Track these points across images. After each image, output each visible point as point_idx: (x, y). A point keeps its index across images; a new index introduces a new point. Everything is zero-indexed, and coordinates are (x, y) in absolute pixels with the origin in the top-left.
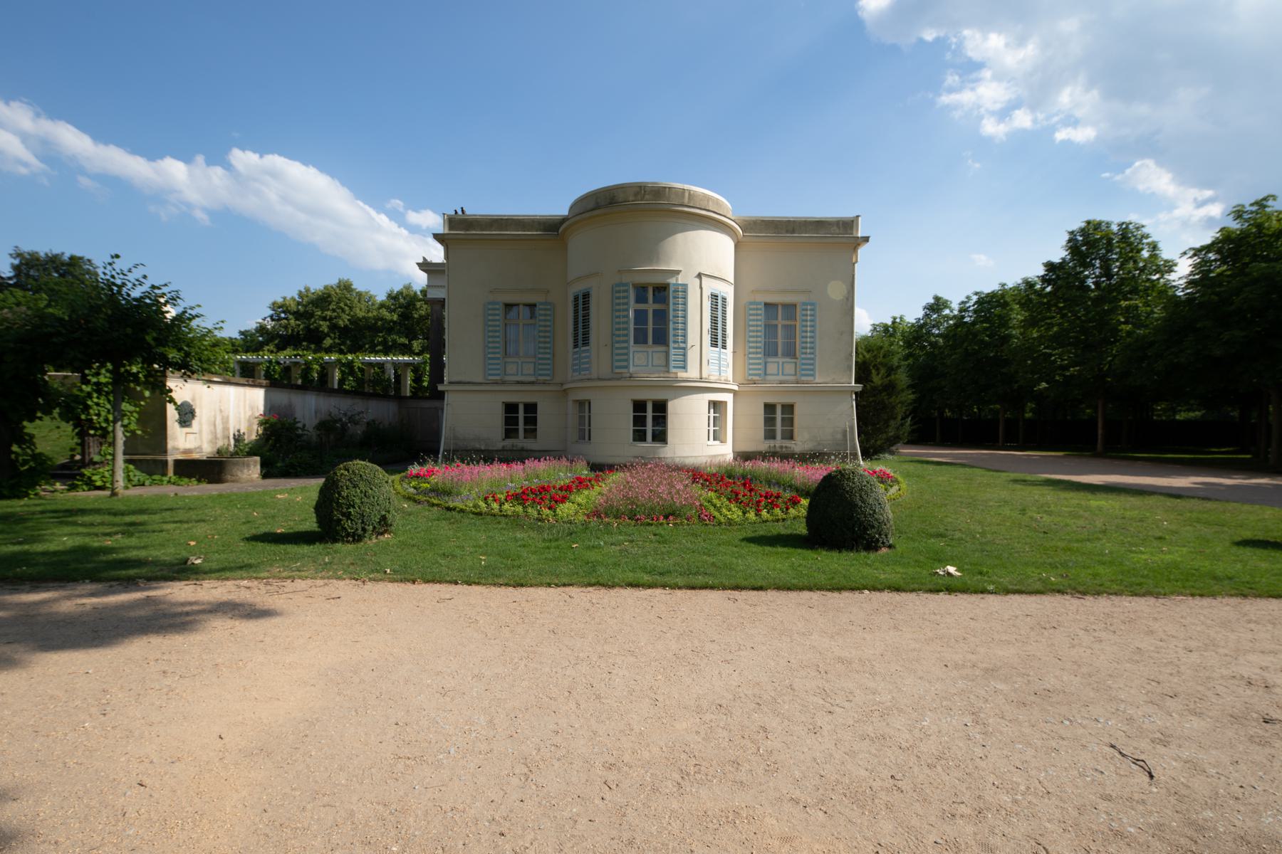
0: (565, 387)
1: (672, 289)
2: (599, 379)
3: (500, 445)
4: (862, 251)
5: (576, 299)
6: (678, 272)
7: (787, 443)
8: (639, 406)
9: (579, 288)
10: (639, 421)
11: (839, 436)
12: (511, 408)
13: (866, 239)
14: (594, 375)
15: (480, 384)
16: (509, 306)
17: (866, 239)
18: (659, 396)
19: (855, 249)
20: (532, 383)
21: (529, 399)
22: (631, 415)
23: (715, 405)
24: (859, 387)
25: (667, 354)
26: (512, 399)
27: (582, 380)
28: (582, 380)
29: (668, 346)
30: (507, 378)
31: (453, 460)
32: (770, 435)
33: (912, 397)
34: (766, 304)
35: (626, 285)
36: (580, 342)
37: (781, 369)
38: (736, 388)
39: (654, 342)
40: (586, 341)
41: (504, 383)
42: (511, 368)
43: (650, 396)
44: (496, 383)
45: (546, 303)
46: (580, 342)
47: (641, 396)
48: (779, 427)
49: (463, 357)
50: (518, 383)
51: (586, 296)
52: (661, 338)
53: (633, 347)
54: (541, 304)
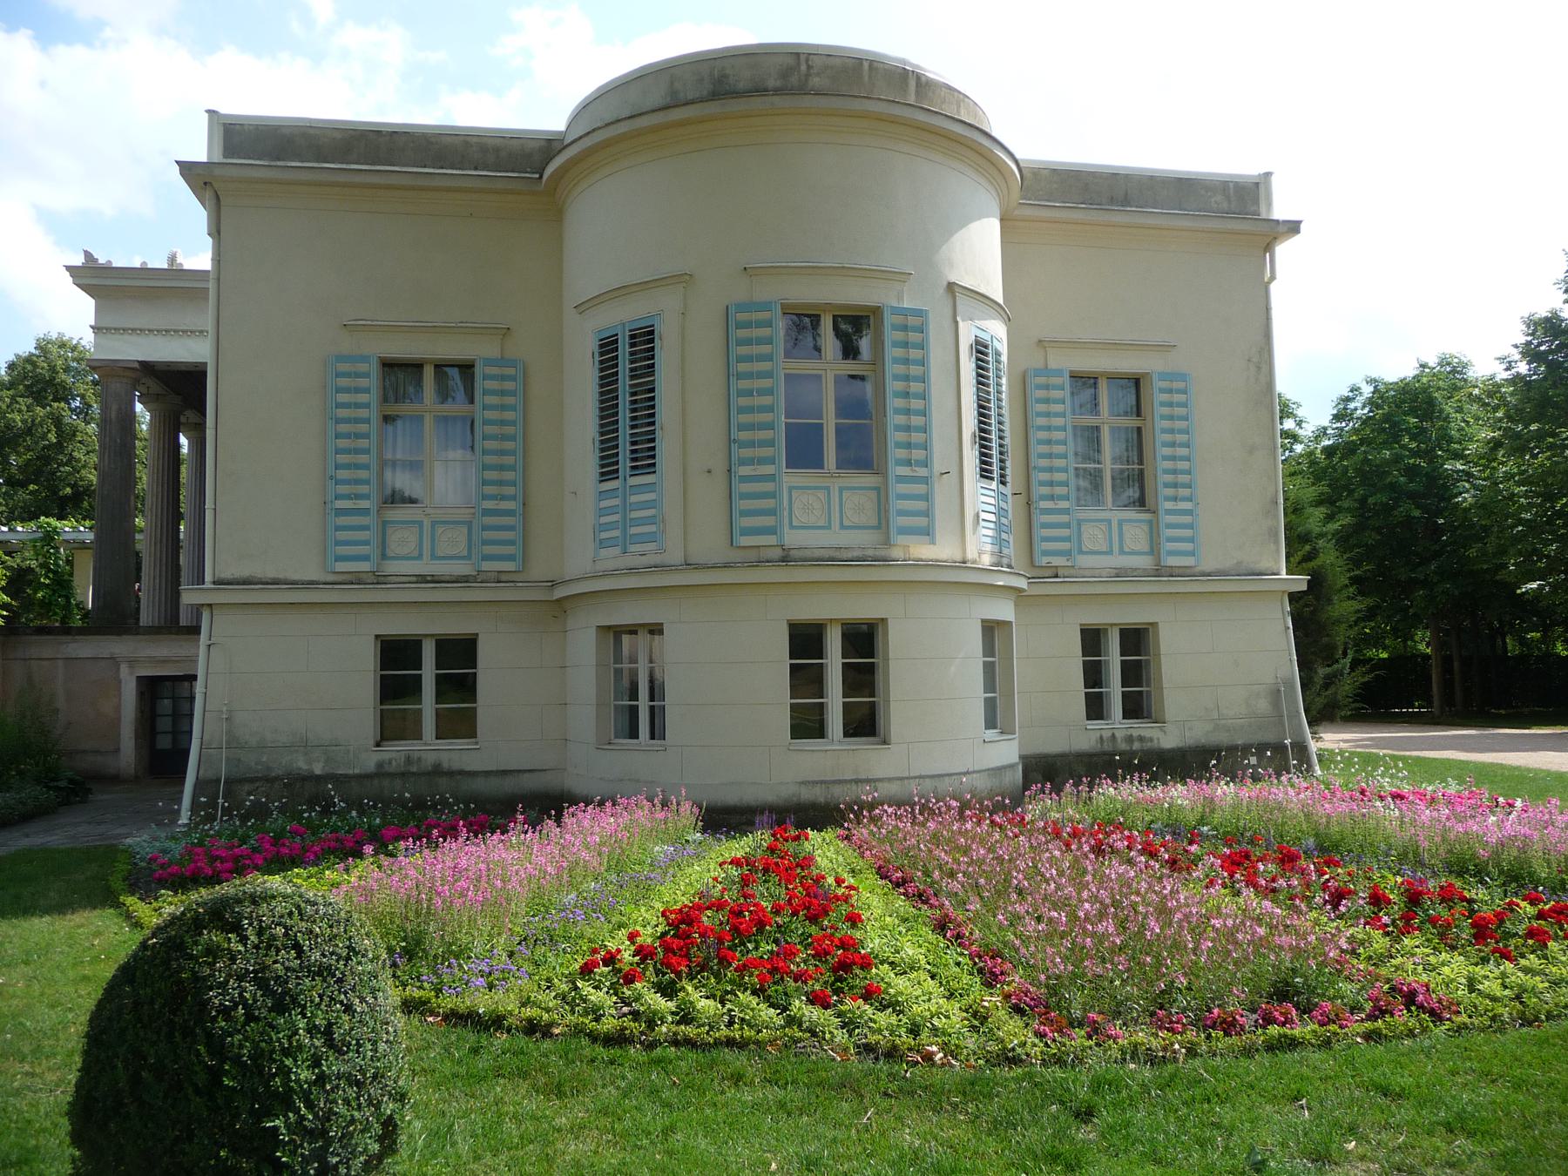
0: (560, 593)
1: (889, 320)
2: (689, 565)
3: (369, 760)
4: (1284, 251)
5: (608, 346)
6: (904, 276)
7: (1139, 728)
8: (806, 640)
9: (620, 317)
10: (806, 679)
11: (1263, 705)
12: (397, 655)
13: (1293, 227)
14: (675, 556)
15: (311, 584)
16: (390, 366)
17: (1293, 227)
18: (861, 609)
19: (1269, 247)
20: (465, 579)
21: (1134, 616)
22: (787, 662)
23: (991, 629)
24: (1300, 582)
25: (882, 495)
26: (1094, 618)
27: (632, 571)
28: (632, 571)
29: (882, 472)
30: (392, 567)
31: (359, 855)
32: (1096, 708)
33: (1354, 605)
34: (1076, 377)
35: (765, 306)
36: (625, 463)
37: (1109, 539)
38: (1022, 583)
39: (842, 464)
40: (645, 459)
41: (380, 579)
42: (402, 541)
43: (834, 607)
44: (356, 580)
45: (502, 362)
46: (625, 463)
47: (810, 610)
48: (1115, 690)
49: (261, 503)
50: (422, 579)
51: (644, 339)
52: (861, 452)
53: (793, 479)
54: (490, 362)
